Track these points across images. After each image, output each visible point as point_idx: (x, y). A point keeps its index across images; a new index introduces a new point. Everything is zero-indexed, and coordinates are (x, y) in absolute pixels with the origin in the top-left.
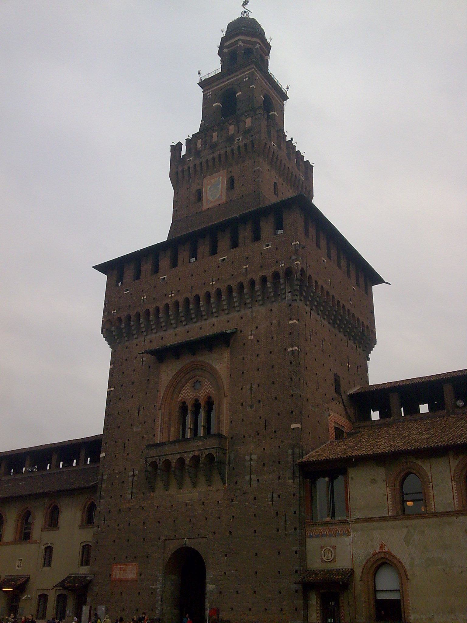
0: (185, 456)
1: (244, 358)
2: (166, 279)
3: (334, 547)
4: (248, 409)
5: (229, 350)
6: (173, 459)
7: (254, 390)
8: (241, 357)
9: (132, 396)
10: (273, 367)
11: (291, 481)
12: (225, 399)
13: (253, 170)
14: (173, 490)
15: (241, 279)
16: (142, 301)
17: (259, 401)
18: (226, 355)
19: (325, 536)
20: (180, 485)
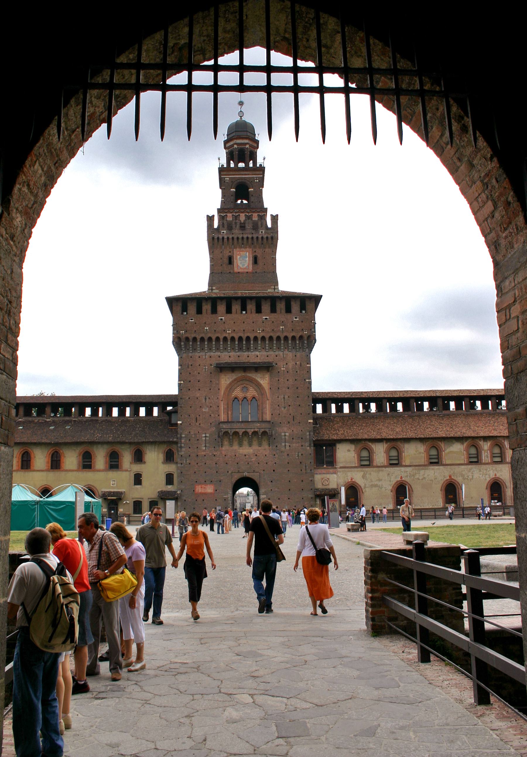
0: (248, 430)
1: (279, 380)
2: (223, 320)
3: (328, 479)
4: (283, 409)
5: (269, 373)
6: (241, 432)
7: (286, 399)
8: (277, 379)
9: (199, 389)
10: (297, 388)
11: (308, 448)
12: (267, 401)
13: (272, 256)
14: (236, 447)
15: (278, 334)
16: (205, 330)
17: (289, 406)
18: (267, 376)
19: (324, 474)
20: (240, 445)
